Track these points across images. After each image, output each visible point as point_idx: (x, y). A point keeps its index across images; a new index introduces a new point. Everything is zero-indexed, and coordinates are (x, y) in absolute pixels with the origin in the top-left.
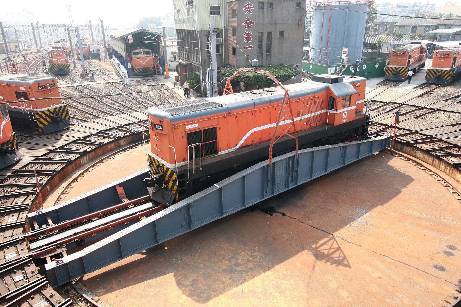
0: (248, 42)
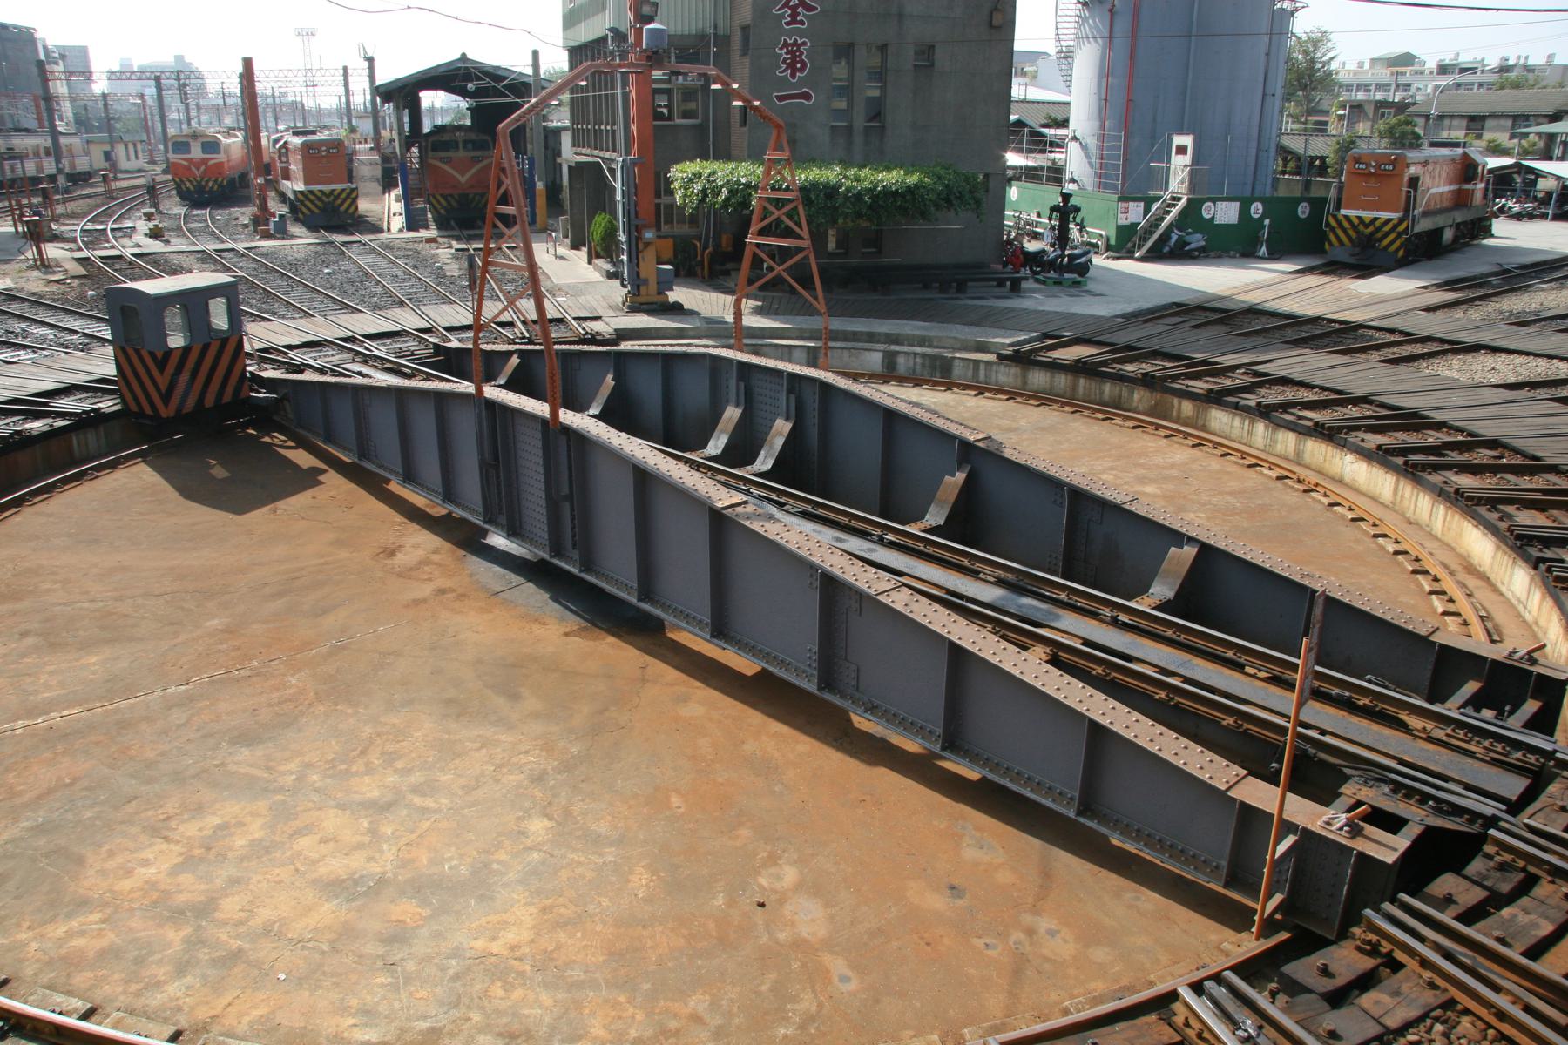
0: (793, 76)
